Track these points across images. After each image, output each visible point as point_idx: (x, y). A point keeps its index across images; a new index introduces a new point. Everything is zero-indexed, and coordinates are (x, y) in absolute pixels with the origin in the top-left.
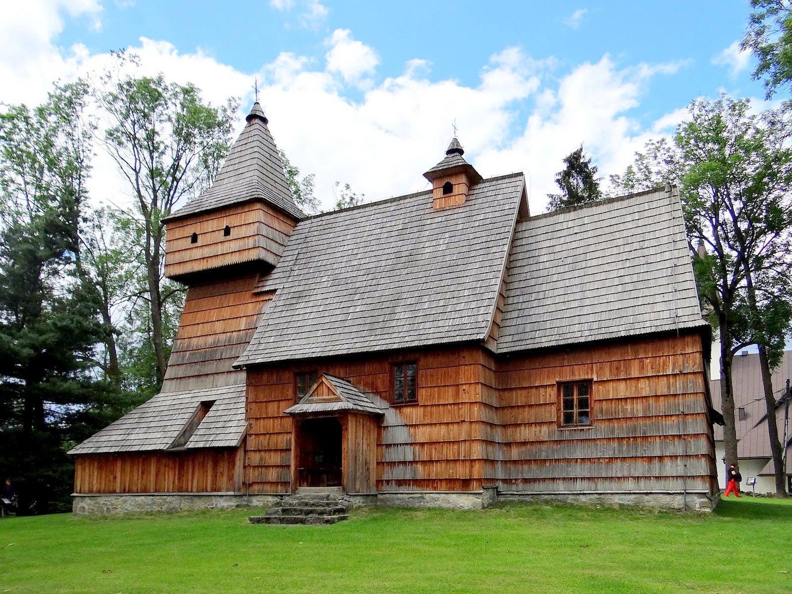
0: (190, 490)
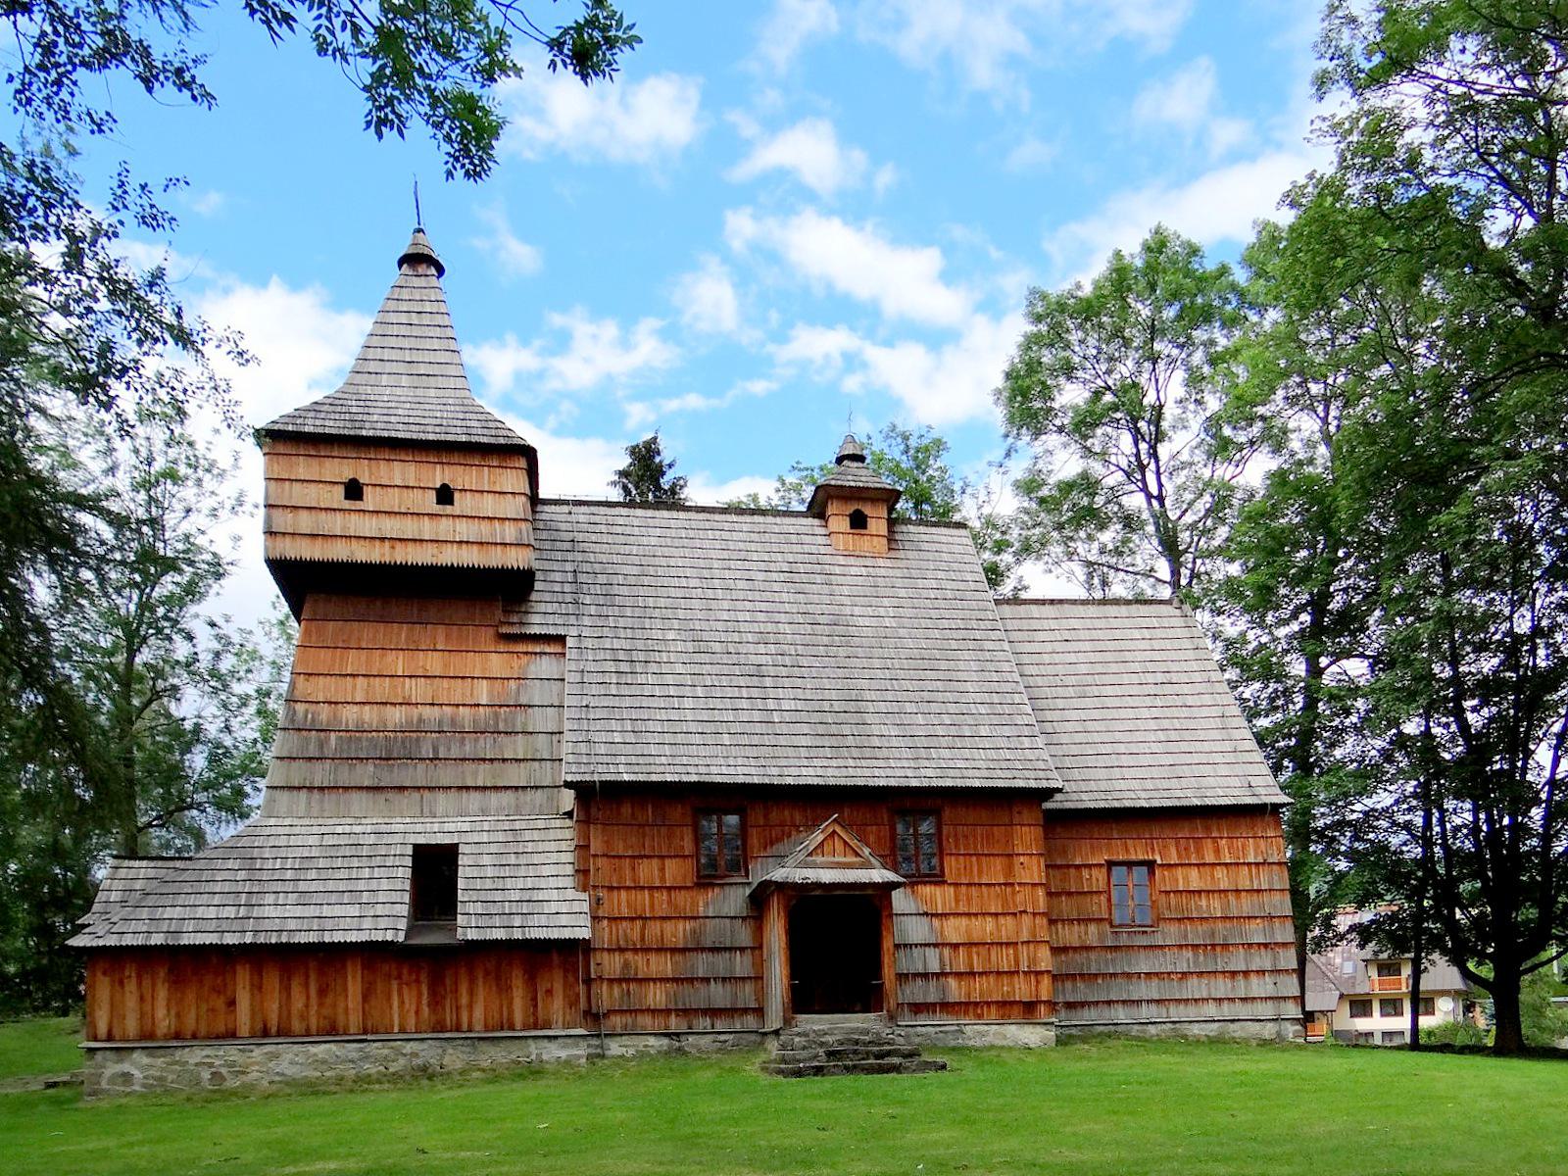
0: (465, 1027)
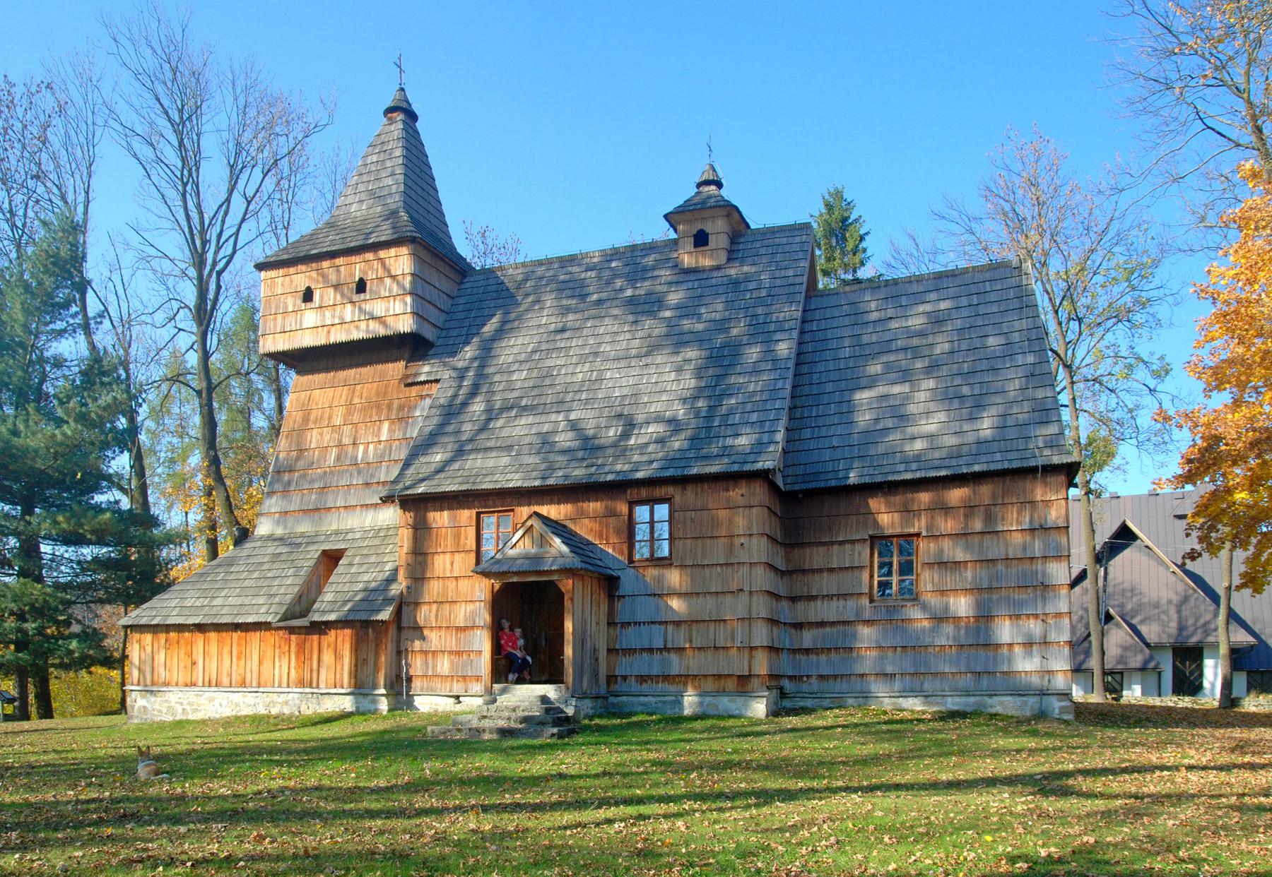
0: (314, 685)
